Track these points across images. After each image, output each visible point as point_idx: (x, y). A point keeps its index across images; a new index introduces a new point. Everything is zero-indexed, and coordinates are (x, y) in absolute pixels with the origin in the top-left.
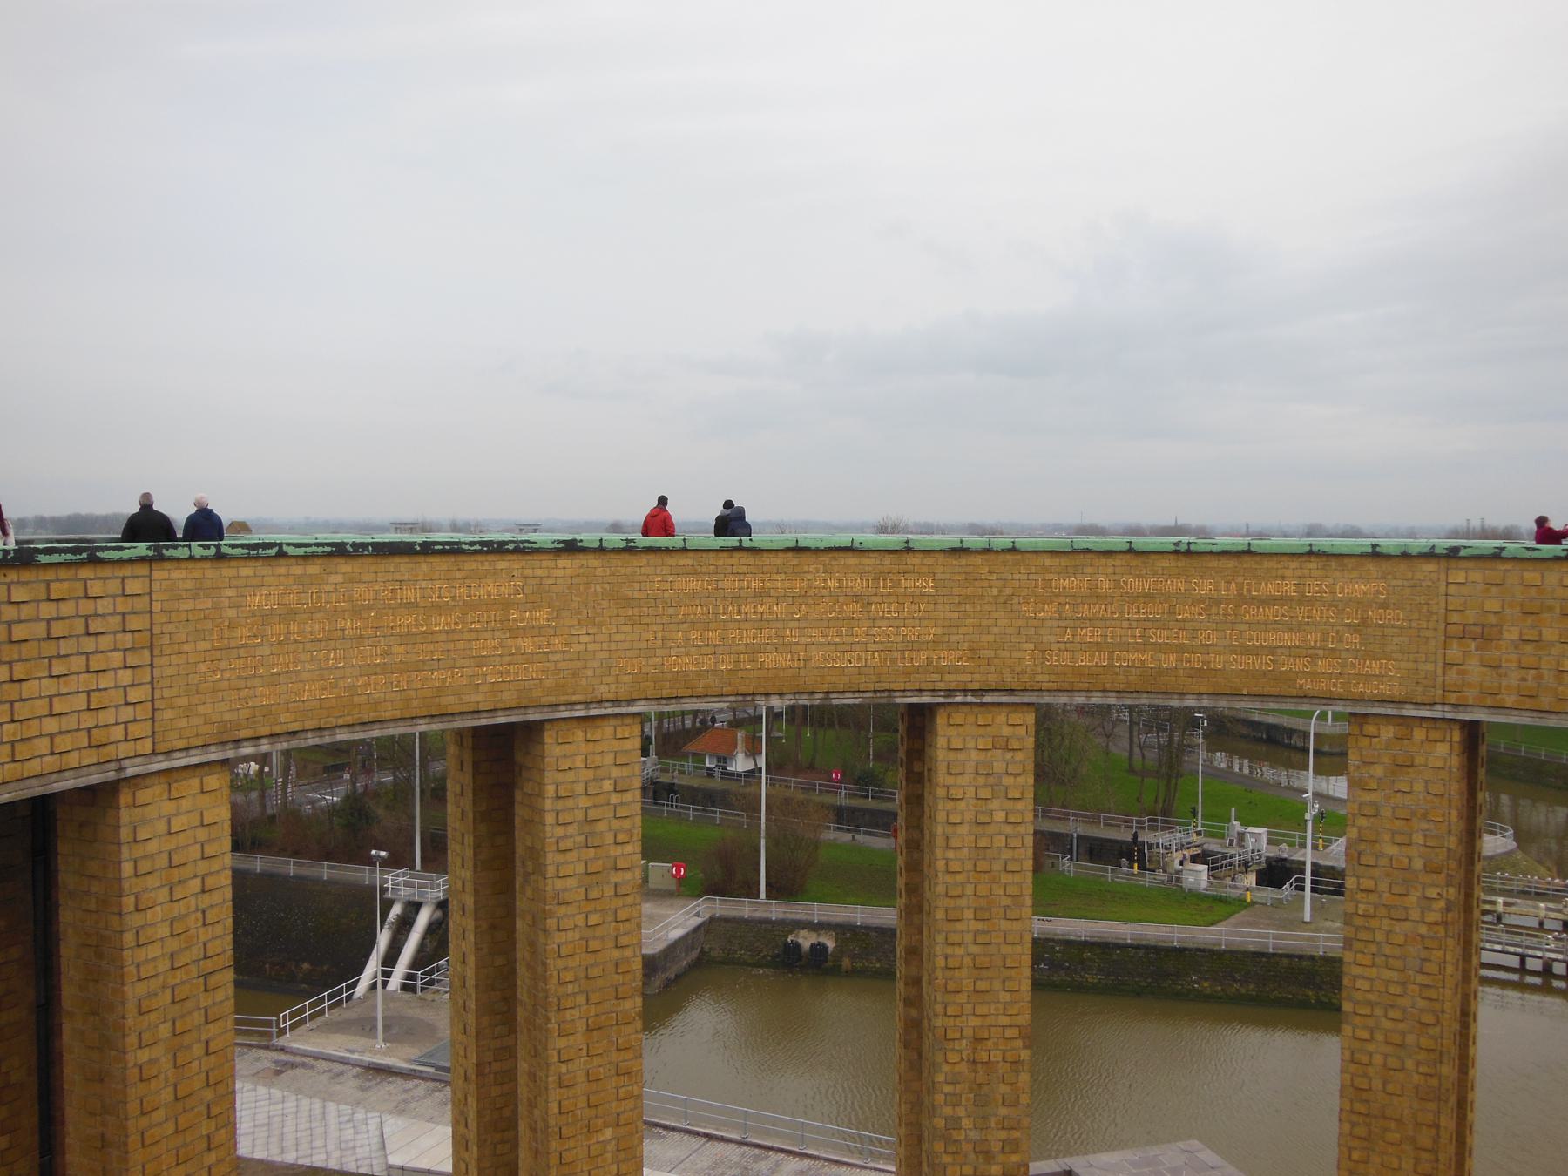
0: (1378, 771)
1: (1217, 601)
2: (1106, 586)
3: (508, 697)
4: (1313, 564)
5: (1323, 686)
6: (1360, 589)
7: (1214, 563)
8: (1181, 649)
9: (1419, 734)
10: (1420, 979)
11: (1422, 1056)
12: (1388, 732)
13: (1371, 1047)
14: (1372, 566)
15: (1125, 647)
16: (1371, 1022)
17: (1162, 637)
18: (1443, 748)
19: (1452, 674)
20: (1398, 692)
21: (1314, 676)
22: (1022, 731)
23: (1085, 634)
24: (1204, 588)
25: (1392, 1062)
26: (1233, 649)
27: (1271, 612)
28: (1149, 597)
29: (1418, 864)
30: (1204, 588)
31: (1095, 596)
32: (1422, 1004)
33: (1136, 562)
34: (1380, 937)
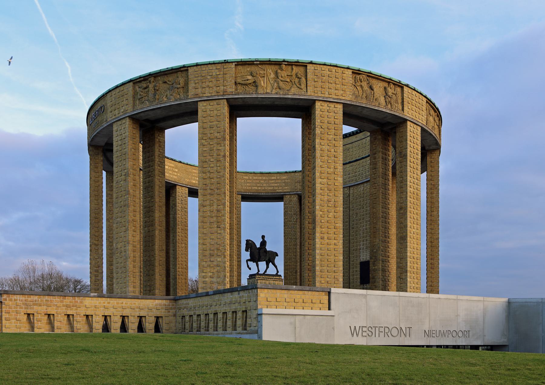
0: (287, 202)
1: (266, 180)
2: (251, 178)
3: (173, 180)
4: (278, 174)
5: (280, 191)
6: (284, 178)
7: (265, 175)
8: (261, 187)
9: (292, 196)
10: (294, 229)
11: (294, 239)
12: (288, 197)
13: (287, 240)
14: (286, 174)
15: (254, 186)
16: (287, 236)
17: (259, 185)
18: (295, 198)
19: (296, 187)
20: (289, 191)
21: (279, 189)
22: (239, 198)
23: (248, 184)
24: (264, 178)
25: (290, 241)
26: (268, 187)
27: (273, 181)
28: (256, 179)
29: (293, 214)
30: (264, 178)
31: (249, 179)
32: (294, 232)
33: (255, 174)
34: (288, 224)
